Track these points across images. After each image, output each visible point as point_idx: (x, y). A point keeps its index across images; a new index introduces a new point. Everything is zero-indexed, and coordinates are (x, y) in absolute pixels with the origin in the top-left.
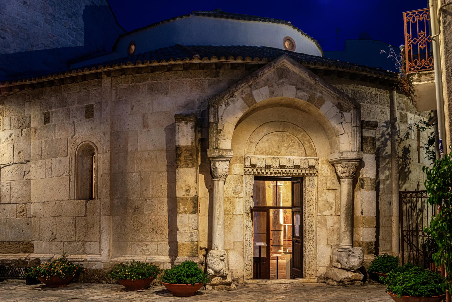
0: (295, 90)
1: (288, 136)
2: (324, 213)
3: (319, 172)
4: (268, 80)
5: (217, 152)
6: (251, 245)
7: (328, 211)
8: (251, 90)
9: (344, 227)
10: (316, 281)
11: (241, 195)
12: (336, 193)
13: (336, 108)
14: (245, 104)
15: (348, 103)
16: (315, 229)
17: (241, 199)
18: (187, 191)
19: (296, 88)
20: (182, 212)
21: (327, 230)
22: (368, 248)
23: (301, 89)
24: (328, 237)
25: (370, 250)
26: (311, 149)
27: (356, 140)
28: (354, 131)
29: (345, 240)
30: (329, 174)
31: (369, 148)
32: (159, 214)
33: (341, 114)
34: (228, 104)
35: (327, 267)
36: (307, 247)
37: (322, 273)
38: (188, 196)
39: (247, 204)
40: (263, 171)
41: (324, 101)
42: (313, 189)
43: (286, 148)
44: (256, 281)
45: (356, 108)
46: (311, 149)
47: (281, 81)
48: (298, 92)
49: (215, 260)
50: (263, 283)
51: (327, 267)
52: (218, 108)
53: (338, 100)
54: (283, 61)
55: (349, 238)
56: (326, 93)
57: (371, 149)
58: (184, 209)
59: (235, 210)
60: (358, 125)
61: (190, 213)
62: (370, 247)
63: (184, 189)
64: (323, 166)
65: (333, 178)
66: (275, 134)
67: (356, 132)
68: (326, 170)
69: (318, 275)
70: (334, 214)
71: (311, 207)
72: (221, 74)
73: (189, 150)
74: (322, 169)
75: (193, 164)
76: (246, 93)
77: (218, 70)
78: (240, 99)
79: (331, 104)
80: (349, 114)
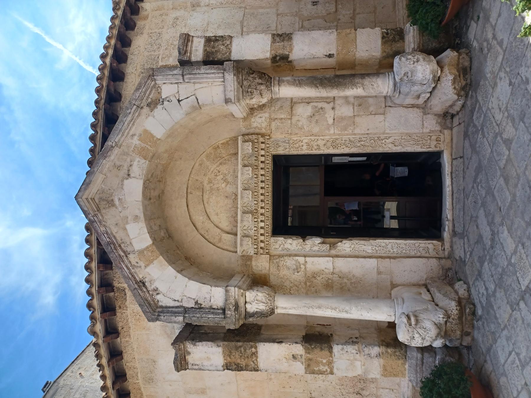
0: (130, 180)
1: (210, 182)
2: (331, 121)
4: (117, 224)
5: (229, 312)
6: (383, 245)
7: (326, 115)
8: (134, 252)
9: (355, 89)
10: (449, 131)
12: (295, 103)
13: (156, 110)
14: (155, 262)
15: (146, 90)
16: (358, 137)
19: (127, 179)
20: (329, 367)
21: (358, 116)
22: (394, 40)
23: (129, 171)
24: (371, 114)
25: (397, 37)
27: (205, 76)
28: (190, 79)
29: (378, 87)
31: (222, 47)
32: (334, 383)
33: (166, 103)
34: (156, 290)
35: (425, 114)
37: (434, 122)
38: (303, 357)
40: (262, 224)
41: (146, 131)
42: (291, 142)
43: (229, 186)
44: (446, 235)
47: (117, 202)
48: (132, 175)
49: (416, 336)
50: (451, 225)
51: (425, 114)
52: (162, 307)
53: (142, 108)
54: (86, 201)
55: (374, 80)
56: (133, 129)
57: (223, 45)
58: (324, 365)
59: (326, 271)
60: (181, 72)
61: (331, 356)
62: (391, 38)
63: (291, 362)
64: (255, 125)
65: (273, 108)
66: (208, 203)
67: (192, 76)
69: (438, 128)
70: (332, 104)
71: (321, 143)
72: (120, 285)
73: (230, 352)
74: (259, 126)
76: (139, 261)
77: (115, 290)
78: (148, 269)
79: (150, 118)
80: (164, 87)
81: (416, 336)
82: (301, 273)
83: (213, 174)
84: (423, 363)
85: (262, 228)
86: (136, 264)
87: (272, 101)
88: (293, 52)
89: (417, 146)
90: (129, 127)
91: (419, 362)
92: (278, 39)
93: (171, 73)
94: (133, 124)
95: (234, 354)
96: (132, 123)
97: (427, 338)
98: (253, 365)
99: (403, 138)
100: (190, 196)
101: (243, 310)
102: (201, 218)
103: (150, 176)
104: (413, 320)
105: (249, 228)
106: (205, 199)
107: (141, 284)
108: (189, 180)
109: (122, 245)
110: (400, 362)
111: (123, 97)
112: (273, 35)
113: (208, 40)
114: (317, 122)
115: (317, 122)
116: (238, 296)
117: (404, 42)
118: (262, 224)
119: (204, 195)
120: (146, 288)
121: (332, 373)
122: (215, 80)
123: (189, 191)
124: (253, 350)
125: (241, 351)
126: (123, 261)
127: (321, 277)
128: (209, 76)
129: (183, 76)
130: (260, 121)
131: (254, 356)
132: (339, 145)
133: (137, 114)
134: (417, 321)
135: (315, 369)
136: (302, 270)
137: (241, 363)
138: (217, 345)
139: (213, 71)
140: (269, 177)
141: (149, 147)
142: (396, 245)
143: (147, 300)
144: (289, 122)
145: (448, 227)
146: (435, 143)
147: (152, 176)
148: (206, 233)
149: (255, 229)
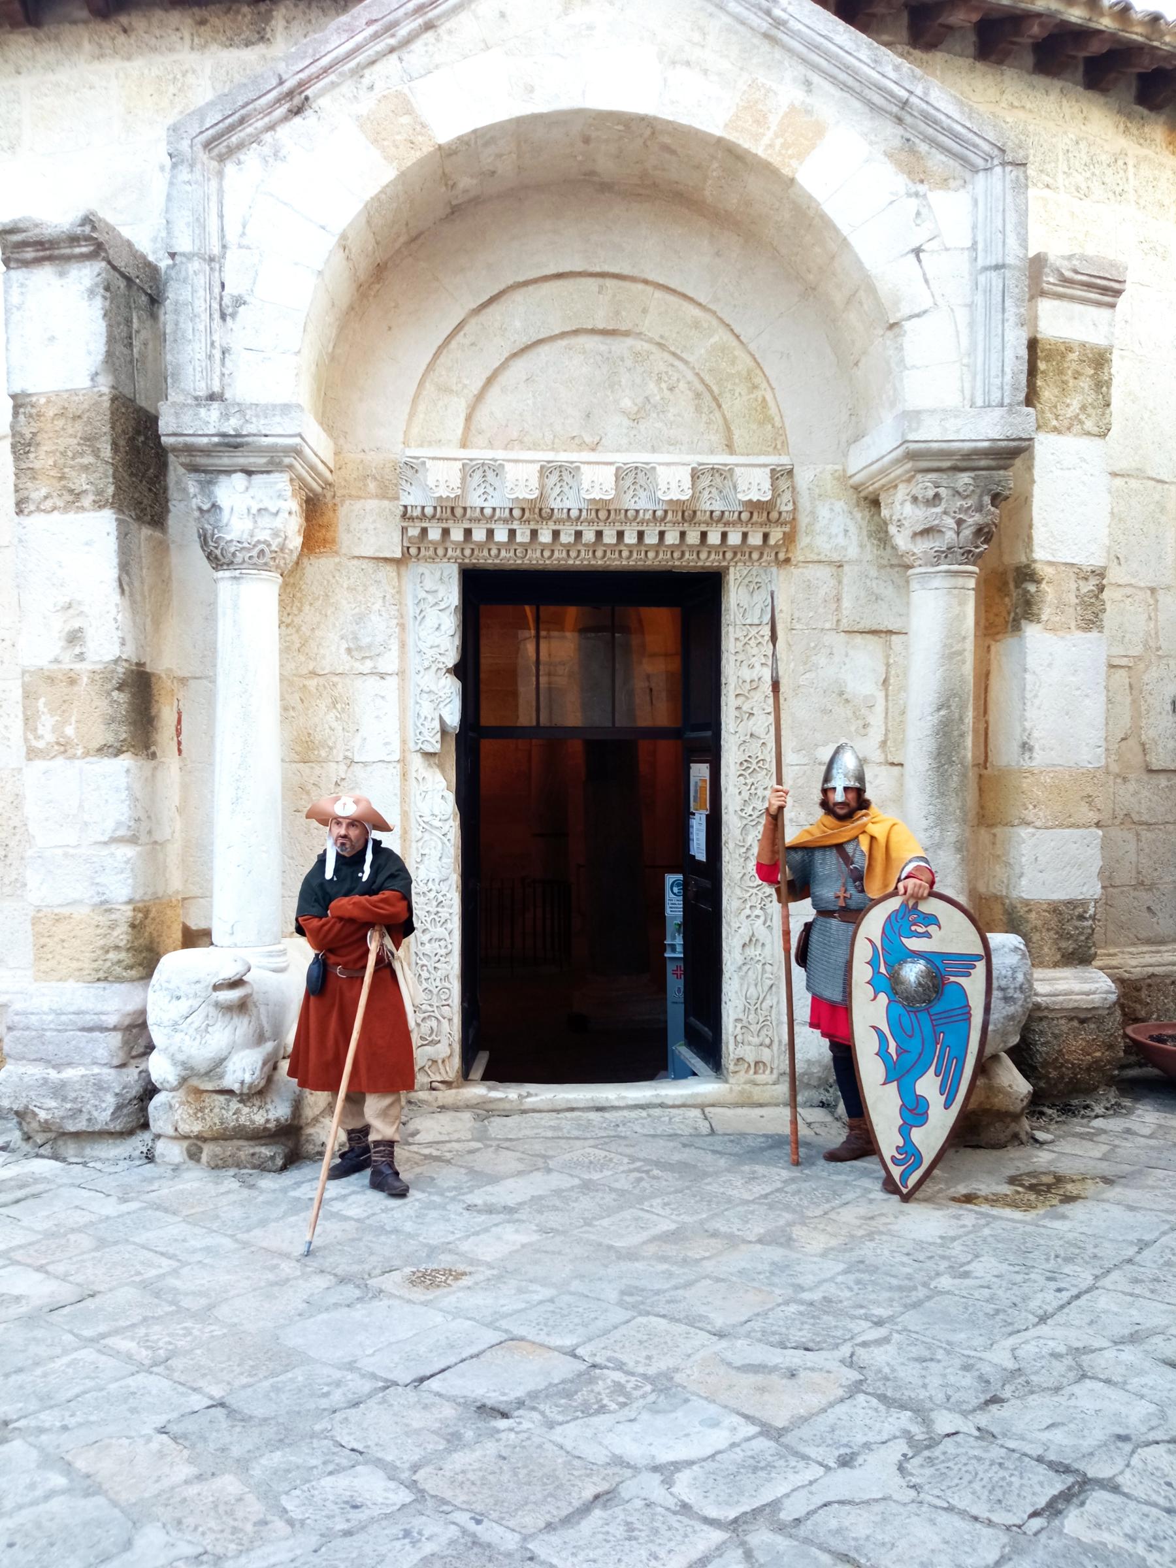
3: (803, 540)
6: (444, 914)
11: (389, 662)
17: (392, 682)
18: (74, 637)
26: (761, 424)
28: (988, 291)
30: (853, 552)
33: (913, 203)
36: (735, 925)
38: (78, 666)
39: (427, 709)
40: (501, 536)
41: (819, 130)
43: (626, 422)
44: (478, 1091)
45: (1003, 164)
46: (761, 424)
56: (827, 86)
57: (1083, 408)
58: (57, 728)
59: (357, 742)
60: (1010, 260)
61: (87, 754)
64: (823, 512)
65: (873, 572)
68: (834, 530)
74: (818, 527)
75: (100, 493)
81: (183, 1006)
82: (344, 663)
83: (662, 367)
84: (90, 1029)
85: (490, 533)
86: (366, 81)
87: (902, 565)
88: (1048, 635)
89: (741, 1007)
90: (836, 71)
91: (89, 1020)
92: (1089, 586)
93: (1009, 227)
94: (844, 87)
95: (71, 431)
96: (850, 81)
97: (178, 1037)
98: (36, 496)
99: (768, 967)
100: (592, 284)
101: (225, 461)
102: (518, 324)
103: (667, 140)
104: (233, 995)
105: (490, 490)
106: (582, 340)
107: (297, 100)
108: (646, 282)
109: (429, 36)
110: (87, 965)
111: (925, 56)
112: (1100, 573)
113: (1100, 360)
114: (826, 711)
115: (826, 711)
116: (273, 449)
117: (1056, 965)
118: (501, 536)
119: (597, 338)
120: (285, 119)
121: (32, 754)
122: (979, 377)
123: (609, 283)
124: (87, 501)
125: (82, 454)
126: (376, 36)
127: (334, 725)
128: (995, 356)
129: (997, 267)
130: (834, 530)
131: (70, 498)
132: (749, 781)
133: (877, 99)
134: (229, 1009)
135: (41, 702)
136: (357, 665)
137: (42, 455)
138: (97, 374)
139: (1008, 370)
140: (653, 561)
141: (766, 140)
142: (443, 952)
143: (242, 121)
144: (828, 626)
145: (501, 1100)
146: (751, 1058)
147: (666, 148)
148: (467, 342)
149: (488, 512)
